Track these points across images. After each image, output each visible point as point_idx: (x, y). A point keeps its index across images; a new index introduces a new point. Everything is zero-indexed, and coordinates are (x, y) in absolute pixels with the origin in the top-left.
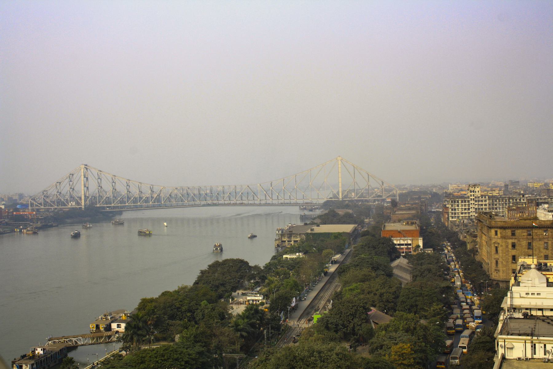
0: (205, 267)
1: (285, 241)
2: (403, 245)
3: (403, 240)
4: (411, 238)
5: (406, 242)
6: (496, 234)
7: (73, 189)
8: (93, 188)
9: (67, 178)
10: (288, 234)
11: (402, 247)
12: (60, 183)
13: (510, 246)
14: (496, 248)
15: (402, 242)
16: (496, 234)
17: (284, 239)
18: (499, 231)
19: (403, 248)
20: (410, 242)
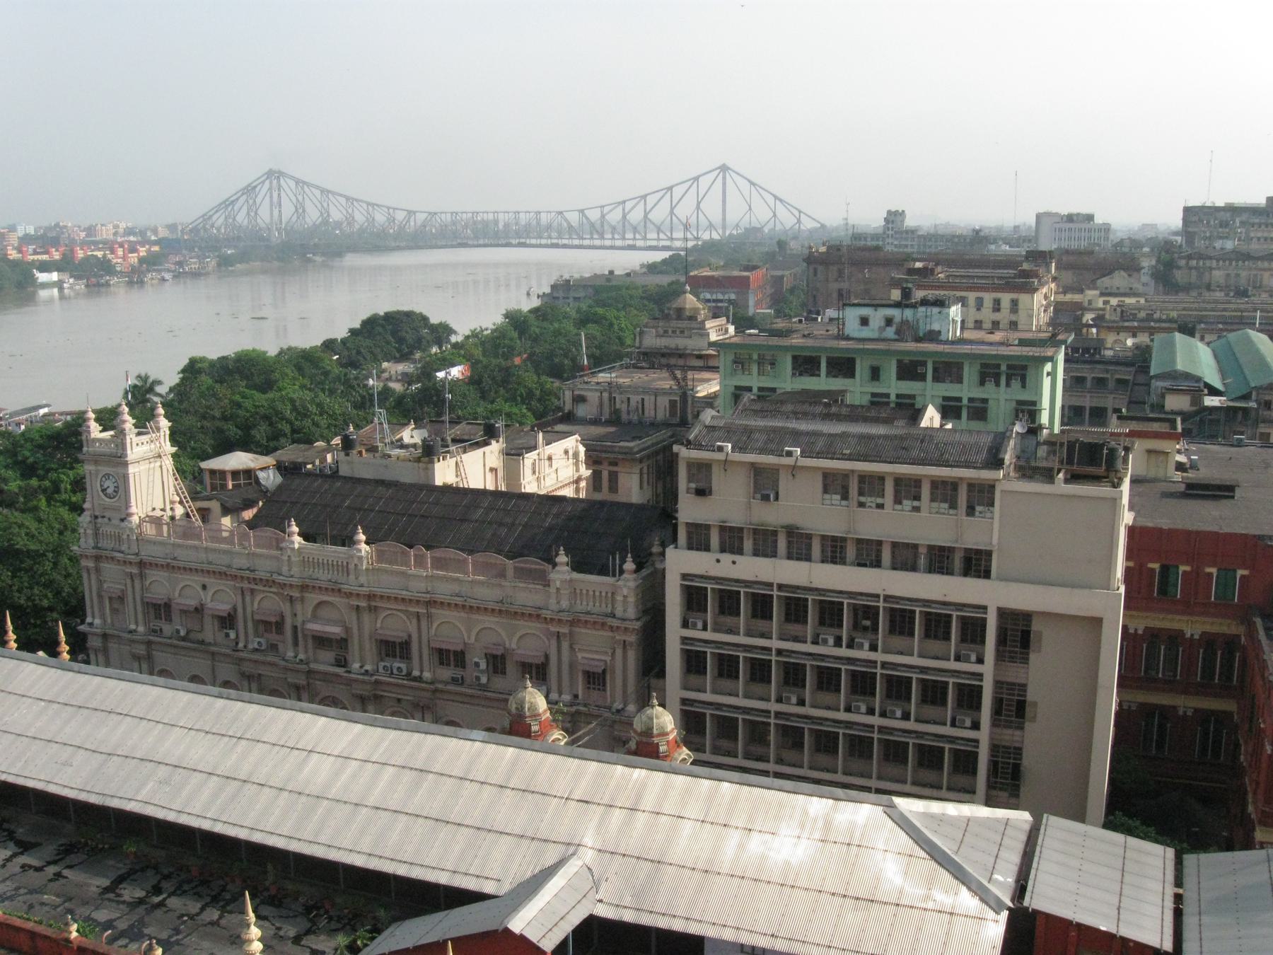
0: (357, 325)
1: (558, 298)
2: (721, 301)
3: (722, 293)
4: (735, 290)
5: (726, 297)
6: (815, 274)
7: (256, 213)
8: (313, 216)
9: (243, 194)
10: (562, 285)
11: (720, 304)
12: (233, 202)
13: (835, 295)
14: (815, 297)
15: (720, 297)
16: (815, 274)
17: (555, 295)
18: (820, 268)
19: (721, 307)
20: (733, 297)
